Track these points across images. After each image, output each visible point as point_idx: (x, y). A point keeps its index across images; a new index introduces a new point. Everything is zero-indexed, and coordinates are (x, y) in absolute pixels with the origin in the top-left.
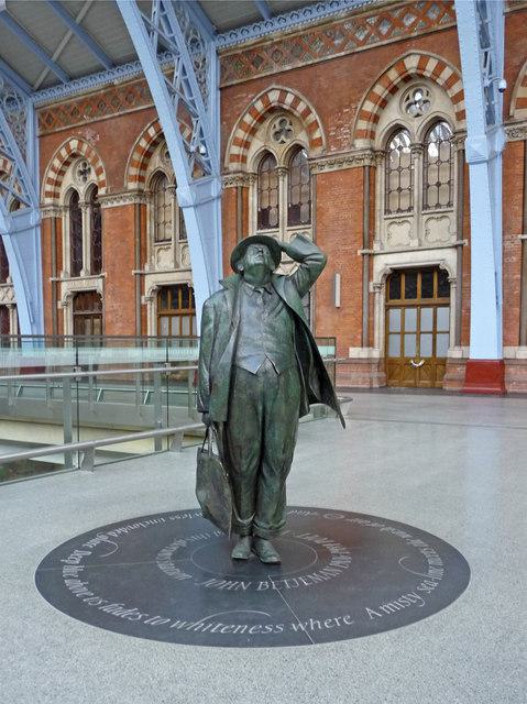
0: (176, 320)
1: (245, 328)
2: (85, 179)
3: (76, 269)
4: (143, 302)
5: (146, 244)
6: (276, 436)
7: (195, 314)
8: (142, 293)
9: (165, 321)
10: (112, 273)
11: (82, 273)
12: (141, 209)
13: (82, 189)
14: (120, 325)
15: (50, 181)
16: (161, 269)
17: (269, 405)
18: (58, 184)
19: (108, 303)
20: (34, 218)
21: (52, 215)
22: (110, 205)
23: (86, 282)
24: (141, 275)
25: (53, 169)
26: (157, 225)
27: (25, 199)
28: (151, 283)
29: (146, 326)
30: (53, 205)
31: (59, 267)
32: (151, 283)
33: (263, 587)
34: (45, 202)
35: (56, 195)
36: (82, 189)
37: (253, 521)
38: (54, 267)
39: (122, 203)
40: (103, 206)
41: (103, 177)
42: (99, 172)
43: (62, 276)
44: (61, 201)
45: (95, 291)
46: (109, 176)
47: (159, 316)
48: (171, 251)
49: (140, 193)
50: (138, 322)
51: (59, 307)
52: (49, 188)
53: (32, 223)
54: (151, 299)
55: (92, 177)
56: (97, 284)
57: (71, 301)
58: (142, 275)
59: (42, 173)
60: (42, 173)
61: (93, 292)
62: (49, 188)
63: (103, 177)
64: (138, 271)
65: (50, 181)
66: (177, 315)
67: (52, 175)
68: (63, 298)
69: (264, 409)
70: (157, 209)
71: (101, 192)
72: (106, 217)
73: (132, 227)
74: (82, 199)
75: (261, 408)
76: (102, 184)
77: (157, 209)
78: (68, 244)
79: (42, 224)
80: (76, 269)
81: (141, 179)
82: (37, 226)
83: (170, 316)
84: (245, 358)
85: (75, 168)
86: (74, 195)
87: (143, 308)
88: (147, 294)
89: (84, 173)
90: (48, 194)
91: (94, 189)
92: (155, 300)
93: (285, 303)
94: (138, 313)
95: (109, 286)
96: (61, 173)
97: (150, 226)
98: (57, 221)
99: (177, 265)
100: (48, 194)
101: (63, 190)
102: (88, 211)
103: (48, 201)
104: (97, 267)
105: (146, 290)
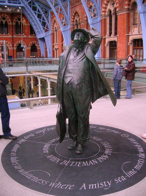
0: (138, 51)
1: (69, 65)
2: (113, 6)
3: (110, 34)
4: (128, 44)
5: (130, 26)
6: (79, 108)
7: (142, 49)
8: (128, 41)
9: (135, 50)
10: (120, 35)
11: (112, 35)
12: (128, 15)
13: (112, 9)
14: (121, 52)
15: (103, 8)
16: (134, 34)
17: (74, 96)
18: (106, 8)
19: (119, 45)
20: (99, 19)
21: (104, 18)
22: (120, 14)
23: (113, 38)
24: (128, 36)
25: (104, 4)
26: (134, 20)
27: (96, 14)
28: (131, 38)
29: (129, 52)
30: (104, 15)
31: (105, 34)
32: (131, 38)
33: (64, 163)
34: (102, 14)
35: (105, 12)
36: (112, 9)
37: (77, 136)
38: (104, 34)
39: (123, 13)
40: (118, 14)
41: (118, 5)
42: (117, 4)
43: (106, 36)
44: (107, 14)
45: (115, 41)
46: (119, 5)
47: (134, 49)
48: (138, 28)
49: (128, 9)
50: (127, 51)
51: (105, 46)
52: (103, 10)
53: (98, 21)
54: (131, 44)
55: (115, 5)
56: (115, 39)
57: (109, 44)
58: (128, 36)
59: (101, 5)
60: (101, 5)
61: (115, 41)
62: (103, 10)
63: (118, 5)
64: (127, 35)
65: (103, 8)
66: (139, 49)
67: (104, 6)
68: (106, 43)
69: (73, 97)
70: (134, 14)
71: (117, 10)
72: (119, 18)
73: (126, 20)
74: (112, 12)
75: (71, 97)
76: (118, 7)
77: (134, 14)
78: (108, 26)
79: (101, 21)
80: (110, 34)
81: (129, 5)
82: (100, 21)
83: (137, 49)
84: (66, 77)
85: (110, 3)
86: (110, 11)
87: (128, 46)
88: (130, 42)
89: (113, 4)
90: (103, 12)
91: (115, 9)
92: (132, 44)
93: (86, 56)
94: (127, 48)
95: (119, 39)
96: (107, 5)
97: (131, 20)
98: (105, 20)
99: (139, 32)
100: (103, 12)
101: (107, 10)
102: (114, 16)
103: (103, 14)
104: (116, 34)
105: (130, 41)
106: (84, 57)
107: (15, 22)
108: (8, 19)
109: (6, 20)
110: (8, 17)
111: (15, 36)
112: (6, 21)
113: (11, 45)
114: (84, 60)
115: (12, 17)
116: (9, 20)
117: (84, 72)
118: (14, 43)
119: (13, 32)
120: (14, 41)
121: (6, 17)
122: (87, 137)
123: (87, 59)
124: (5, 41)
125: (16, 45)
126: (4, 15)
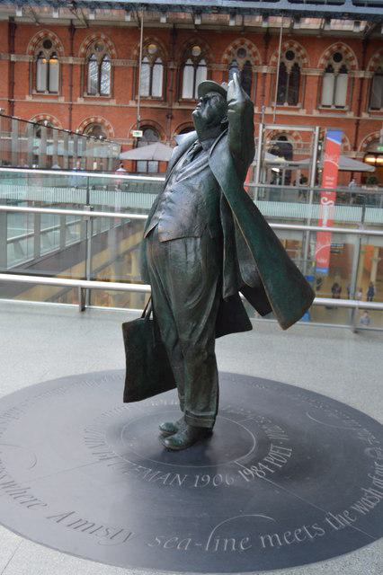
106: (204, 166)
107: (372, 69)
108: (352, 59)
109: (249, 59)
110: (351, 54)
111: (365, 116)
112: (248, 62)
113: (348, 144)
114: (203, 175)
115: (364, 52)
116: (355, 62)
117: (196, 207)
118: (359, 138)
119: (360, 101)
120: (360, 132)
121: (346, 52)
122: (207, 409)
123: (211, 175)
124: (317, 128)
125: (365, 146)
126: (340, 48)
